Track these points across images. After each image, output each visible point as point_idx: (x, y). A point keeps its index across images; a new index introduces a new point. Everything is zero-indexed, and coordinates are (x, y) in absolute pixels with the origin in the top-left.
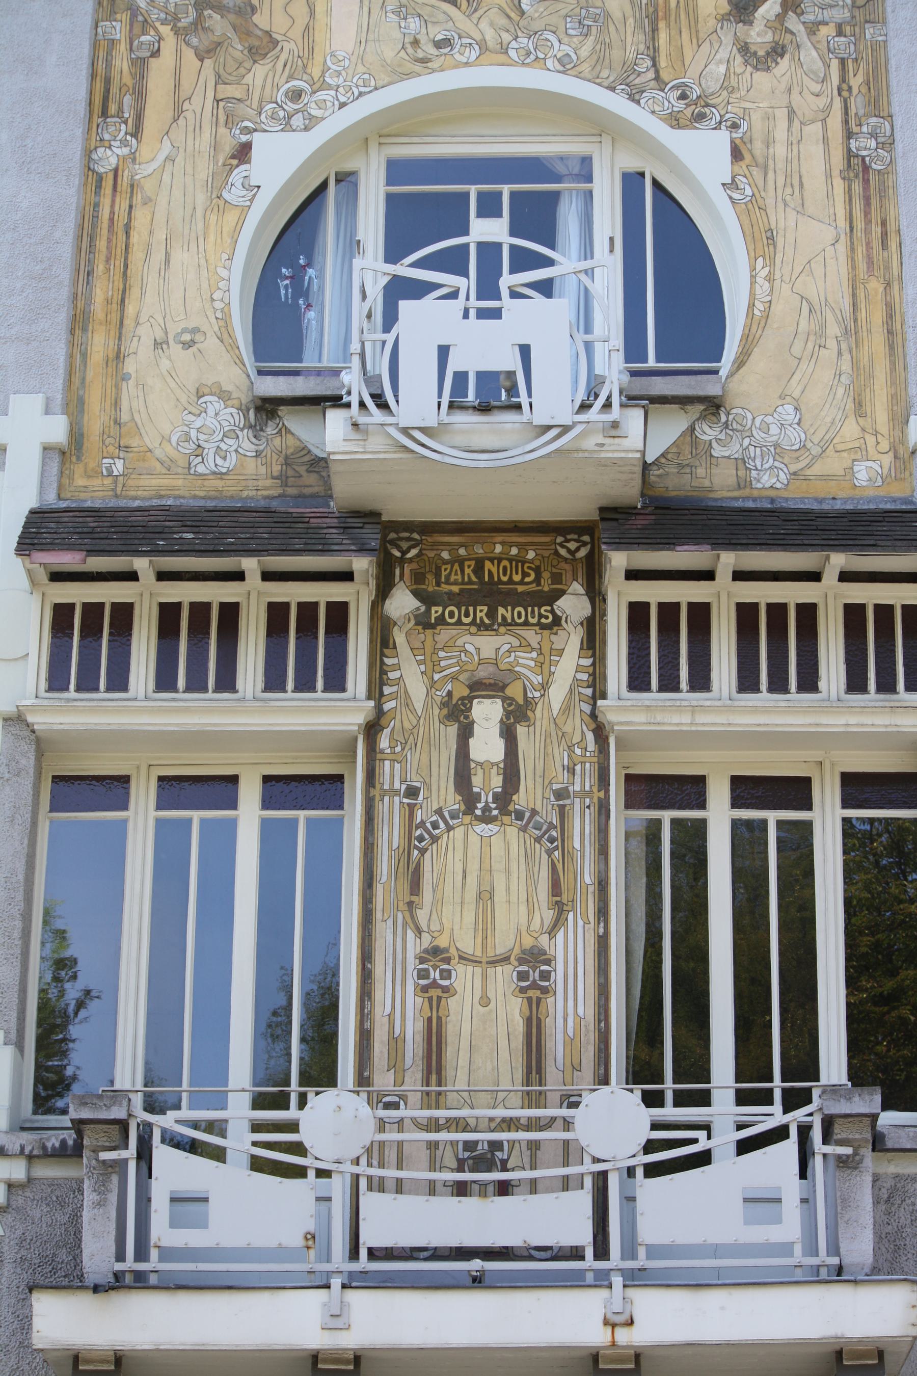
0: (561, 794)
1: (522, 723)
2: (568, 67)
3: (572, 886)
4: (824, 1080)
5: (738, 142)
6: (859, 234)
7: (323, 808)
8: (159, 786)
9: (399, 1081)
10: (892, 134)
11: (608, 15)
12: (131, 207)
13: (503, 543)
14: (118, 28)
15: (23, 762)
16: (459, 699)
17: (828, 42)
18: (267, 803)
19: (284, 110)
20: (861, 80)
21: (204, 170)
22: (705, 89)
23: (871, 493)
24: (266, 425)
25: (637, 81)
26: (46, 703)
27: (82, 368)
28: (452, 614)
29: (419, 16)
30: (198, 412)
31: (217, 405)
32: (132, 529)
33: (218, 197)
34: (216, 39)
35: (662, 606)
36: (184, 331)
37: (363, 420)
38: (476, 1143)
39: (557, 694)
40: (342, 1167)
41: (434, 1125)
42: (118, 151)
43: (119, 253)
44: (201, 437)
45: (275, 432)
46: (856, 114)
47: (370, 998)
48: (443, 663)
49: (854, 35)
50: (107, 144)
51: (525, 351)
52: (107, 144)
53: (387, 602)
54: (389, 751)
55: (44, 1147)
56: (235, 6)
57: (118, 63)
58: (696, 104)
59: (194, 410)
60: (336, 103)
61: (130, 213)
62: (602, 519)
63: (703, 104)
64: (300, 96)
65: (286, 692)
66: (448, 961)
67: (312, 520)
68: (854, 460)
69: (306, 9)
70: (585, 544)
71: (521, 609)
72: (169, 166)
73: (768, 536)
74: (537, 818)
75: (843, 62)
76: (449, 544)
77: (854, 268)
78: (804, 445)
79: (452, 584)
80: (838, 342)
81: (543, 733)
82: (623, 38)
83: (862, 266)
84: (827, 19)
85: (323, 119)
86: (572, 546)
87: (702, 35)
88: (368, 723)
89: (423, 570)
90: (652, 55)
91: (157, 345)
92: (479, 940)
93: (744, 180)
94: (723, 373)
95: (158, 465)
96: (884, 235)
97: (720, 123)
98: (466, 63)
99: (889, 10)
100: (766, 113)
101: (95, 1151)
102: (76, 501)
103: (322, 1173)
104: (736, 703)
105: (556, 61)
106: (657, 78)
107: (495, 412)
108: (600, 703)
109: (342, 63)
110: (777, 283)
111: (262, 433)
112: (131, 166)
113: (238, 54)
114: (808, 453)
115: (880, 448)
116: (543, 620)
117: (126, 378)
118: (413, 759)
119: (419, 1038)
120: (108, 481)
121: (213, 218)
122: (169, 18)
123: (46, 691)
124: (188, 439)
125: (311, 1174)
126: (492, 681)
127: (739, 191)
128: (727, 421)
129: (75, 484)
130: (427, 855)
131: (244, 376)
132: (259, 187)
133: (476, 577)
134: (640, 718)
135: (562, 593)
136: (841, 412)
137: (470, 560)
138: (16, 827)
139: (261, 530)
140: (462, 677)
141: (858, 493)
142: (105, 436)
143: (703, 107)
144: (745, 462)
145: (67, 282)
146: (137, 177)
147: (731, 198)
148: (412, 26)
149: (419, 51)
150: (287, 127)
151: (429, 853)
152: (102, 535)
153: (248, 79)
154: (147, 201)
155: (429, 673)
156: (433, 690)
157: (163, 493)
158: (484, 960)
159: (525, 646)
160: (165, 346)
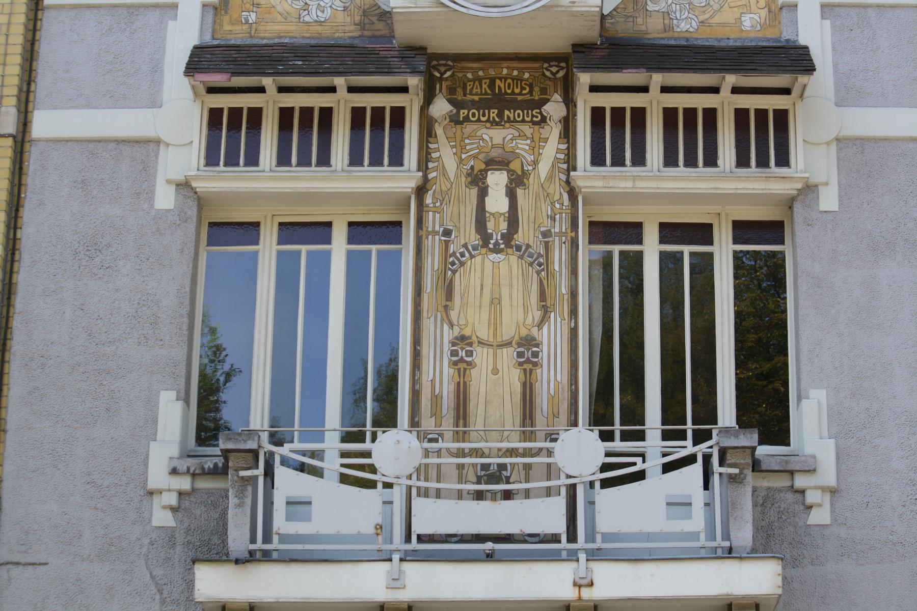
0: (546, 234)
1: (520, 187)
3: (553, 295)
4: (720, 424)
7: (388, 244)
8: (280, 229)
9: (438, 424)
13: (508, 68)
15: (189, 213)
16: (478, 171)
18: (351, 240)
23: (753, 35)
26: (204, 174)
32: (261, 59)
35: (613, 110)
38: (489, 465)
39: (544, 168)
40: (400, 481)
41: (461, 453)
47: (419, 369)
48: (468, 148)
53: (431, 107)
54: (432, 205)
55: (203, 468)
62: (574, 52)
65: (363, 166)
66: (471, 344)
67: (381, 52)
68: (742, 13)
70: (562, 68)
71: (520, 112)
73: (684, 63)
74: (530, 250)
76: (472, 68)
78: (709, 3)
81: (535, 193)
86: (554, 69)
88: (418, 187)
89: (454, 86)
92: (491, 331)
95: (279, 16)
101: (237, 470)
102: (224, 40)
103: (388, 485)
104: (663, 174)
108: (572, 173)
114: (711, 9)
116: (535, 119)
118: (448, 210)
119: (452, 396)
120: (246, 27)
123: (204, 166)
125: (380, 485)
126: (500, 159)
130: (457, 275)
133: (490, 90)
134: (599, 183)
135: (548, 101)
137: (486, 79)
139: (347, 59)
140: (481, 157)
141: (744, 35)
144: (669, 14)
152: (241, 63)
155: (459, 154)
156: (461, 165)
157: (282, 35)
158: (495, 344)
159: (522, 136)
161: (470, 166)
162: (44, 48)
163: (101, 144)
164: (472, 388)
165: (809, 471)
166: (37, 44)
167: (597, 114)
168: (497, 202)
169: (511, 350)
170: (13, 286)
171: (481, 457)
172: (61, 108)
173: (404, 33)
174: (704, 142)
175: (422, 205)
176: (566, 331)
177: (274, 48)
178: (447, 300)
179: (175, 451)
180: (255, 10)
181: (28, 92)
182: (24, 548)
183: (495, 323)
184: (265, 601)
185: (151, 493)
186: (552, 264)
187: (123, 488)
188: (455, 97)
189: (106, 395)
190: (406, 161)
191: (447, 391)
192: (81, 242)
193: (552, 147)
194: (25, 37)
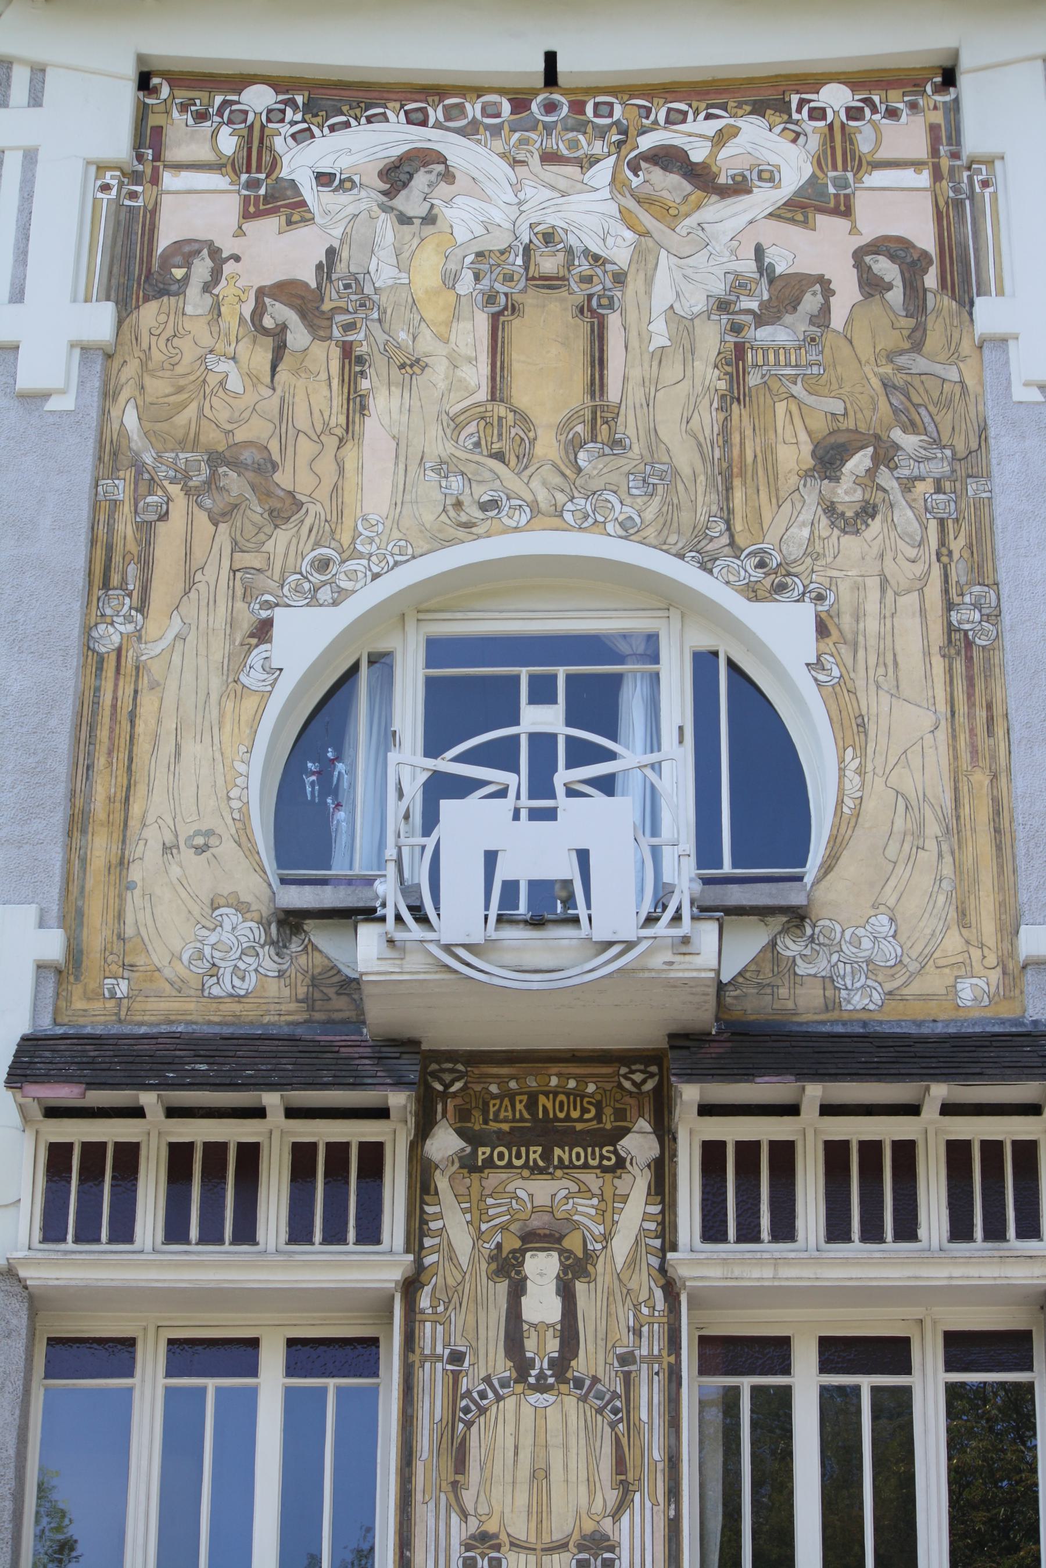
0: (626, 1359)
1: (582, 1279)
2: (632, 531)
5: (823, 615)
6: (962, 719)
7: (355, 1376)
8: (169, 1351)
10: (999, 605)
11: (676, 472)
12: (136, 692)
13: (559, 1075)
14: (121, 487)
15: (14, 1321)
16: (510, 1253)
17: (926, 501)
18: (291, 1370)
19: (310, 581)
20: (963, 543)
21: (219, 651)
22: (787, 556)
23: (976, 1014)
24: (290, 941)
25: (709, 548)
26: (39, 1255)
27: (81, 875)
28: (501, 1156)
29: (463, 474)
30: (212, 926)
31: (234, 918)
32: (138, 1059)
33: (235, 681)
36: (197, 833)
37: (399, 936)
39: (621, 1246)
42: (122, 628)
43: (122, 745)
44: (217, 954)
45: (300, 949)
46: (957, 582)
48: (491, 1212)
49: (955, 492)
50: (108, 620)
51: (583, 857)
52: (108, 620)
53: (428, 1142)
54: (430, 1311)
56: (253, 463)
57: (121, 527)
58: (776, 573)
60: (369, 573)
61: (135, 699)
62: (672, 1047)
63: (784, 572)
64: (328, 566)
65: (313, 1244)
66: (497, 1548)
67: (342, 1050)
68: (957, 977)
69: (334, 467)
70: (652, 1075)
72: (179, 645)
73: (860, 1066)
74: (599, 1386)
75: (942, 522)
76: (498, 1076)
77: (956, 758)
78: (901, 961)
79: (501, 1122)
80: (939, 843)
81: (606, 1290)
82: (693, 498)
83: (965, 755)
84: (924, 473)
86: (638, 1077)
87: (783, 494)
88: (406, 1279)
90: (725, 517)
92: (533, 1525)
93: (831, 659)
94: (808, 879)
95: (167, 986)
96: (990, 720)
97: (804, 594)
98: (516, 528)
99: (994, 462)
100: (855, 582)
102: (73, 1026)
104: (825, 1255)
105: (617, 526)
106: (732, 543)
107: (550, 926)
108: (670, 1255)
109: (375, 529)
110: (869, 777)
111: (285, 950)
112: (136, 645)
113: (257, 518)
114: (904, 970)
115: (986, 963)
116: (605, 1162)
117: (131, 886)
118: (458, 1319)
120: (111, 1004)
121: (230, 705)
122: (179, 476)
123: (40, 1242)
124: (201, 957)
126: (547, 1232)
127: (825, 672)
128: (813, 934)
129: (73, 1007)
130: (474, 1429)
131: (265, 885)
132: (281, 670)
134: (715, 1272)
135: (627, 1131)
136: (941, 923)
137: (521, 1094)
138: (7, 1395)
139: (284, 1061)
141: (962, 1014)
142: (107, 953)
143: (784, 576)
145: (63, 777)
146: (143, 658)
147: (816, 680)
148: (454, 485)
149: (462, 514)
150: (313, 601)
151: (476, 1425)
152: (103, 1066)
153: (269, 546)
154: (154, 686)
155: (476, 1224)
156: (480, 1242)
157: (173, 1018)
159: (585, 1191)
160: (175, 851)
161: (495, 1243)
169: (566, 1556)
174: (895, 1199)
175: (414, 1311)
177: (160, 1040)
178: (456, 1473)
180: (126, 974)
183: (539, 1512)
186: (636, 1410)
188: (469, 1125)
190: (385, 1236)
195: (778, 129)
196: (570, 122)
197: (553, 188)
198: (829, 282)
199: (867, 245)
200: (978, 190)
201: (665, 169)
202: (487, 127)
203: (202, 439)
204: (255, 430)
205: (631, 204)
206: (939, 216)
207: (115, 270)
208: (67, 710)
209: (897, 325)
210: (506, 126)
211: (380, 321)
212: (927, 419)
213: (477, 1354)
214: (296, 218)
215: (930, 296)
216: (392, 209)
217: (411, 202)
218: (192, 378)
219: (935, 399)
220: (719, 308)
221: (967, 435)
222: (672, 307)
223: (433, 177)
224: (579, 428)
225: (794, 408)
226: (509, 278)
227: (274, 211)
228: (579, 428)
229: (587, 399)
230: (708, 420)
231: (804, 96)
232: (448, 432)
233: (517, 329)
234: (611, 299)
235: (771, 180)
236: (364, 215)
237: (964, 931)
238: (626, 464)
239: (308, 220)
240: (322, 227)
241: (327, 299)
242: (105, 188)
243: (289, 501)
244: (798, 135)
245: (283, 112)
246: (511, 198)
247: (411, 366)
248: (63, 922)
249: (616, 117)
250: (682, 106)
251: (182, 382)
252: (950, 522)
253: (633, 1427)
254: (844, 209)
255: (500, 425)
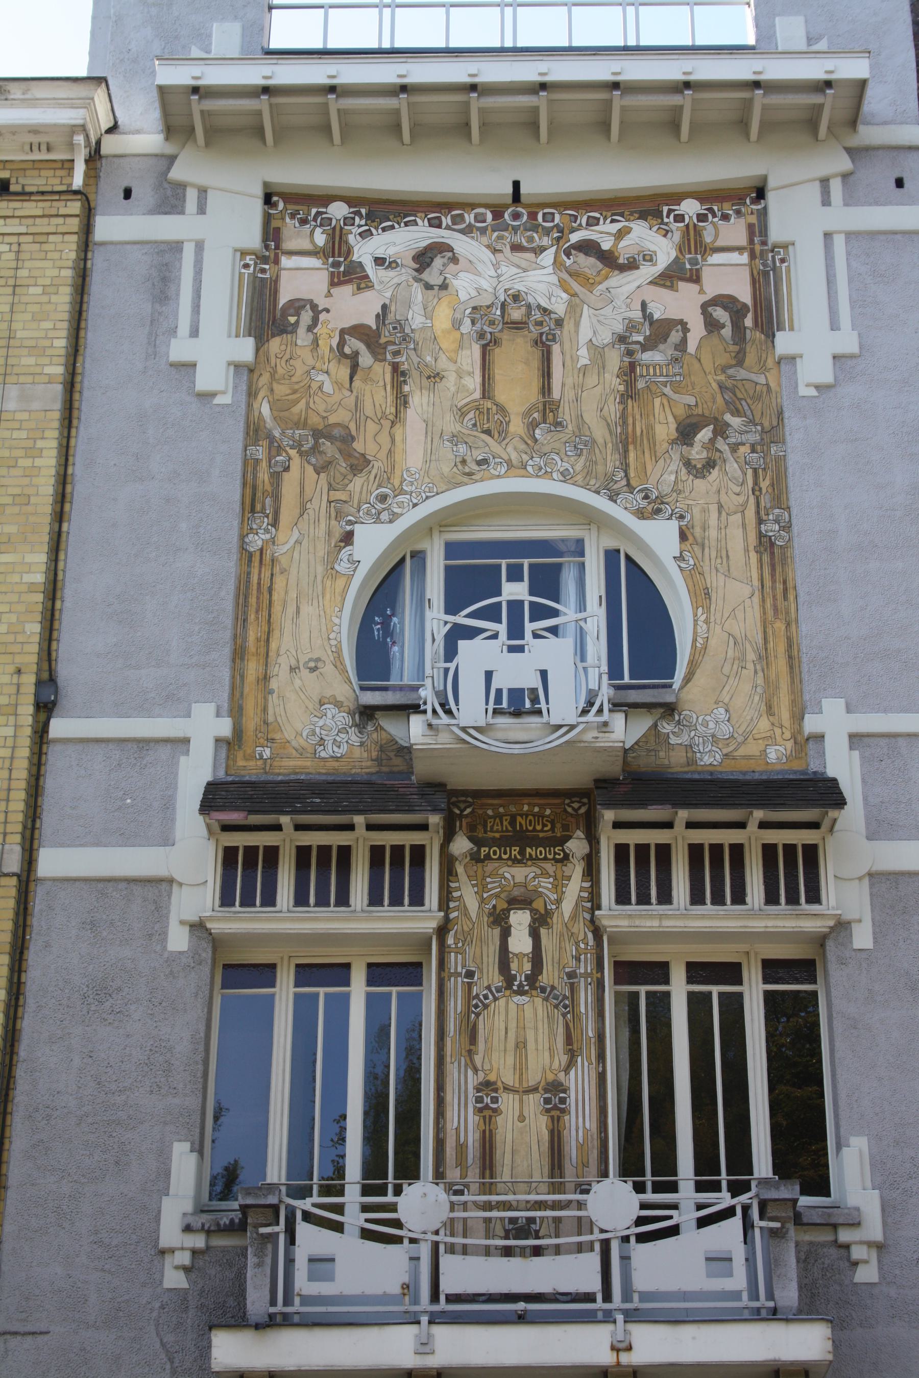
0: (571, 975)
3: (580, 1038)
4: (756, 1175)
5: (684, 528)
8: (296, 972)
10: (790, 521)
11: (594, 441)
12: (272, 575)
13: (529, 804)
15: (204, 955)
18: (370, 982)
23: (778, 767)
25: (614, 487)
26: (219, 914)
29: (466, 443)
31: (333, 711)
34: (327, 459)
36: (311, 660)
37: (435, 722)
38: (517, 1218)
39: (567, 907)
41: (487, 1206)
42: (263, 537)
44: (323, 732)
46: (765, 507)
51: (544, 674)
55: (218, 1224)
59: (318, 715)
61: (271, 579)
62: (597, 788)
66: (496, 1090)
69: (389, 439)
70: (584, 804)
72: (297, 546)
74: (556, 992)
75: (755, 471)
76: (492, 805)
77: (765, 613)
80: (755, 665)
83: (770, 612)
85: (402, 515)
86: (576, 805)
87: (659, 454)
91: (292, 669)
92: (517, 1076)
93: (688, 554)
94: (676, 686)
95: (294, 752)
96: (785, 590)
97: (672, 515)
99: (787, 433)
101: (257, 1226)
102: (238, 776)
103: (413, 1241)
106: (628, 484)
107: (524, 716)
110: (712, 625)
113: (343, 470)
115: (784, 737)
116: (557, 856)
117: (271, 692)
119: (477, 1145)
120: (260, 763)
121: (329, 583)
124: (313, 733)
125: (406, 1241)
130: (481, 1018)
134: (625, 923)
135: (569, 837)
139: (366, 796)
141: (770, 767)
145: (230, 626)
147: (679, 567)
148: (461, 450)
150: (378, 521)
158: (521, 1090)
159: (545, 874)
162: (50, 783)
163: (111, 884)
164: (498, 1136)
165: (853, 1225)
166: (42, 779)
167: (621, 851)
168: (520, 942)
169: (537, 1096)
170: (17, 1033)
171: (509, 1210)
172: (69, 846)
173: (422, 769)
174: (731, 879)
176: (594, 1075)
178: (471, 1044)
179: (189, 1207)
180: (269, 745)
181: (33, 829)
182: (24, 1315)
183: (521, 1068)
184: (287, 1369)
185: (163, 1252)
187: (133, 1247)
189: (115, 1146)
191: (472, 1139)
192: (91, 986)
193: (575, 886)
194: (29, 772)
195: (655, 228)
196: (528, 225)
197: (518, 267)
198: (686, 323)
199: (709, 300)
200: (778, 264)
201: (586, 254)
202: (478, 229)
203: (309, 422)
204: (340, 416)
205: (565, 276)
206: (754, 281)
207: (254, 317)
208: (231, 586)
209: (728, 350)
210: (489, 228)
211: (415, 349)
212: (746, 408)
213: (482, 972)
214: (363, 285)
215: (748, 332)
216: (421, 280)
217: (432, 276)
218: (302, 384)
219: (751, 395)
220: (619, 341)
221: (771, 417)
222: (591, 340)
223: (445, 260)
224: (536, 415)
225: (666, 403)
226: (492, 323)
227: (349, 281)
228: (536, 415)
229: (540, 397)
230: (613, 409)
231: (671, 207)
232: (457, 417)
233: (499, 355)
234: (554, 335)
235: (651, 260)
236: (404, 284)
237: (771, 718)
238: (564, 437)
239: (370, 287)
240: (379, 291)
241: (382, 336)
242: (246, 266)
243: (361, 460)
244: (667, 232)
245: (353, 219)
246: (493, 273)
247: (434, 377)
248: (231, 714)
249: (556, 222)
250: (597, 215)
251: (296, 387)
252: (760, 470)
253: (576, 1016)
254: (695, 278)
255: (488, 413)
